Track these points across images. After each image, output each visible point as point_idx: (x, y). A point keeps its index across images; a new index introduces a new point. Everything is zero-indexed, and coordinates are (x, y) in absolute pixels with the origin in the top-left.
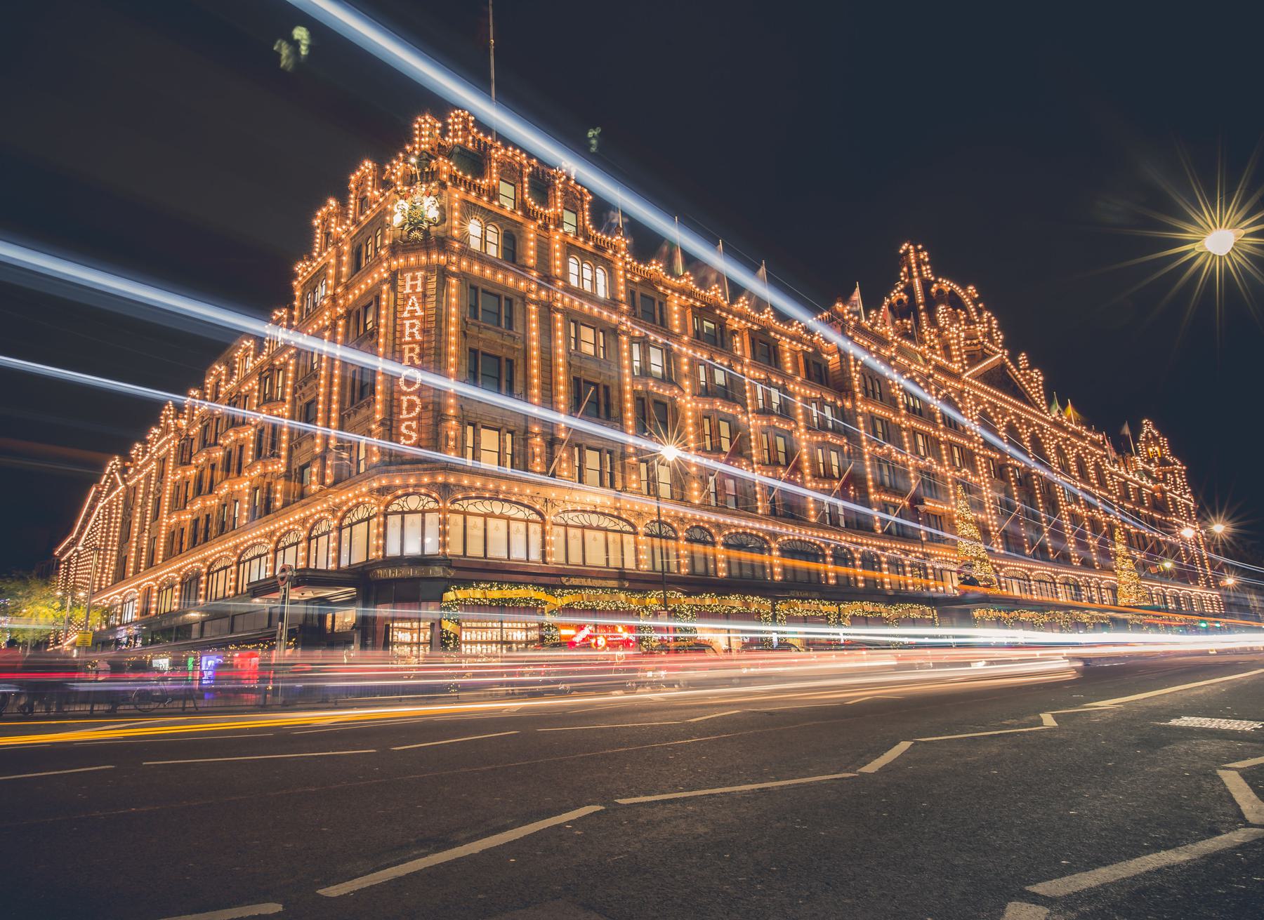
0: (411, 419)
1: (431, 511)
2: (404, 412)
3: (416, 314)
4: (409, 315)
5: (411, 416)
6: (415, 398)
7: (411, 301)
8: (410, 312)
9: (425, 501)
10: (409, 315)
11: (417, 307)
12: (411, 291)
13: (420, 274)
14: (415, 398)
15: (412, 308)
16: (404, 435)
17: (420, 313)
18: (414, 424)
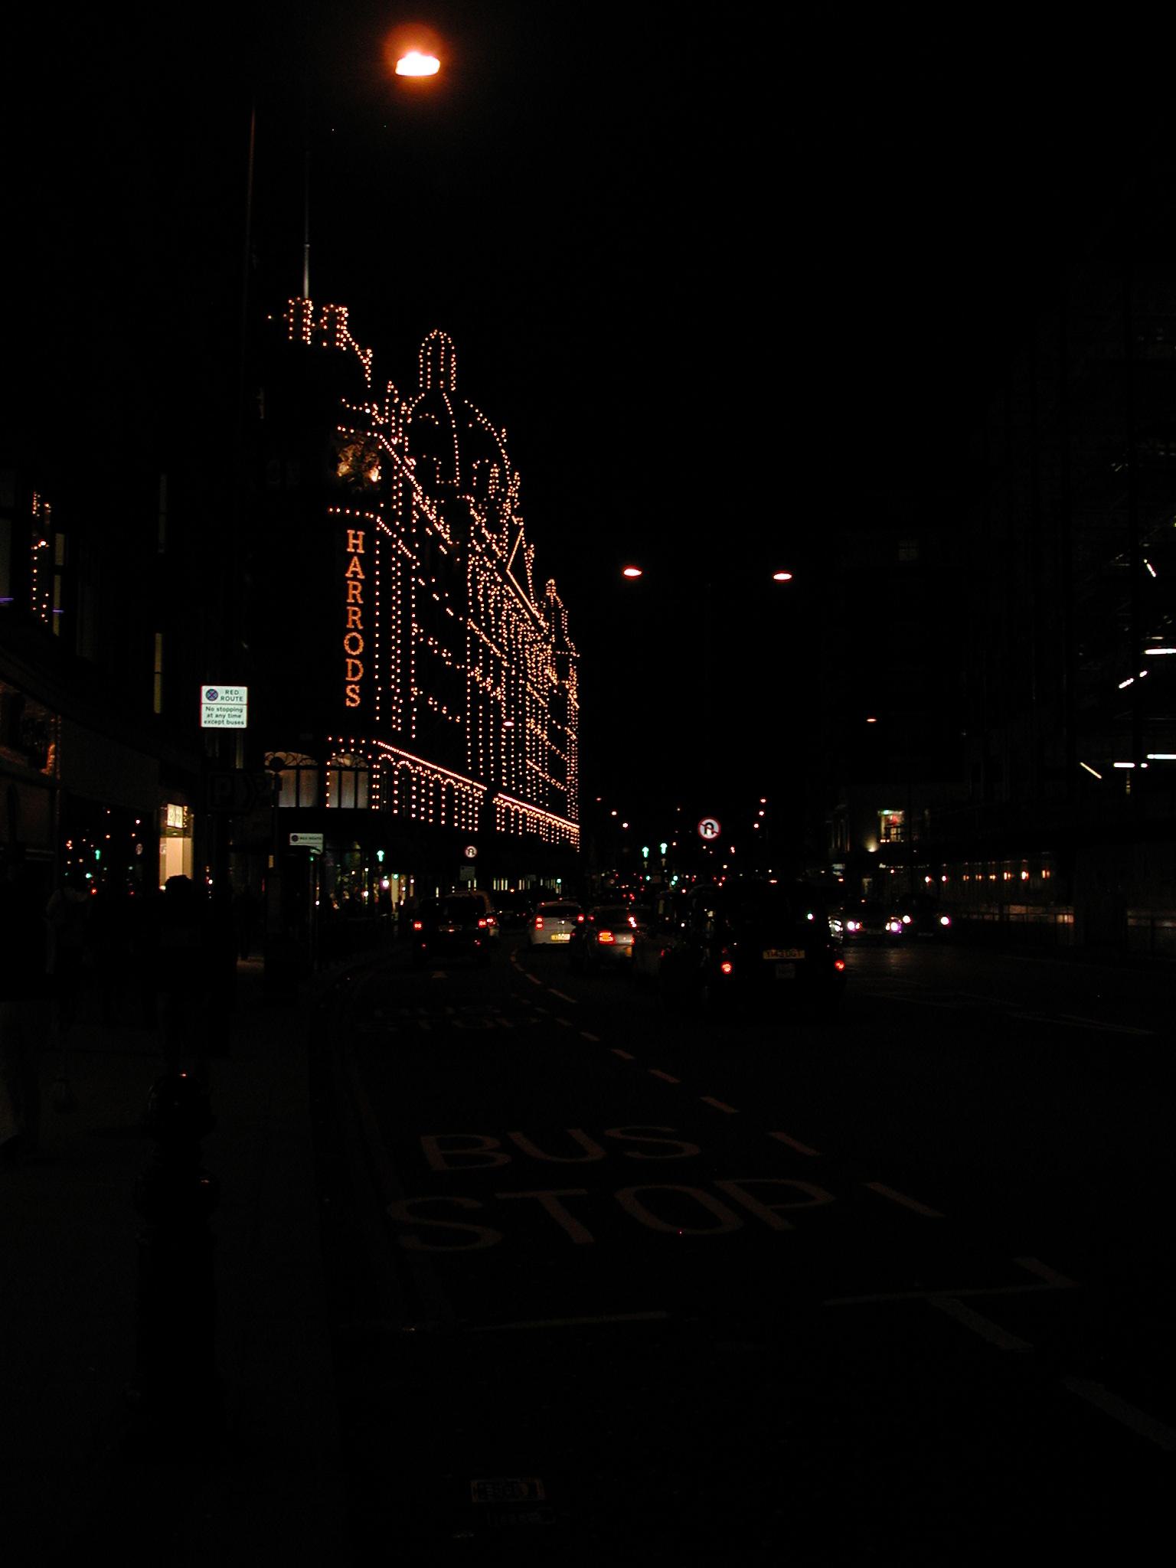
0: (356, 683)
1: (363, 769)
2: (350, 674)
3: (358, 576)
4: (351, 576)
5: (356, 679)
6: (357, 662)
7: (353, 562)
8: (353, 572)
9: (358, 760)
10: (351, 576)
11: (359, 569)
12: (353, 550)
13: (361, 533)
14: (357, 662)
15: (354, 569)
16: (349, 697)
17: (361, 576)
18: (357, 688)
